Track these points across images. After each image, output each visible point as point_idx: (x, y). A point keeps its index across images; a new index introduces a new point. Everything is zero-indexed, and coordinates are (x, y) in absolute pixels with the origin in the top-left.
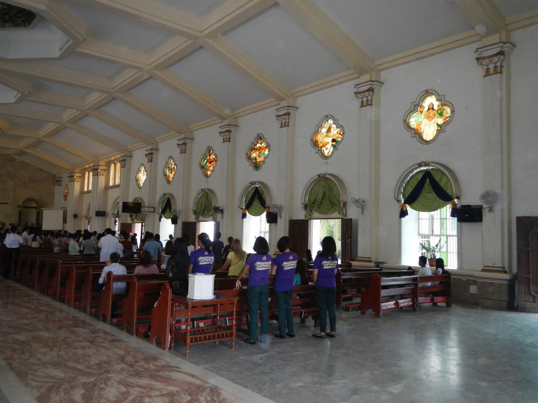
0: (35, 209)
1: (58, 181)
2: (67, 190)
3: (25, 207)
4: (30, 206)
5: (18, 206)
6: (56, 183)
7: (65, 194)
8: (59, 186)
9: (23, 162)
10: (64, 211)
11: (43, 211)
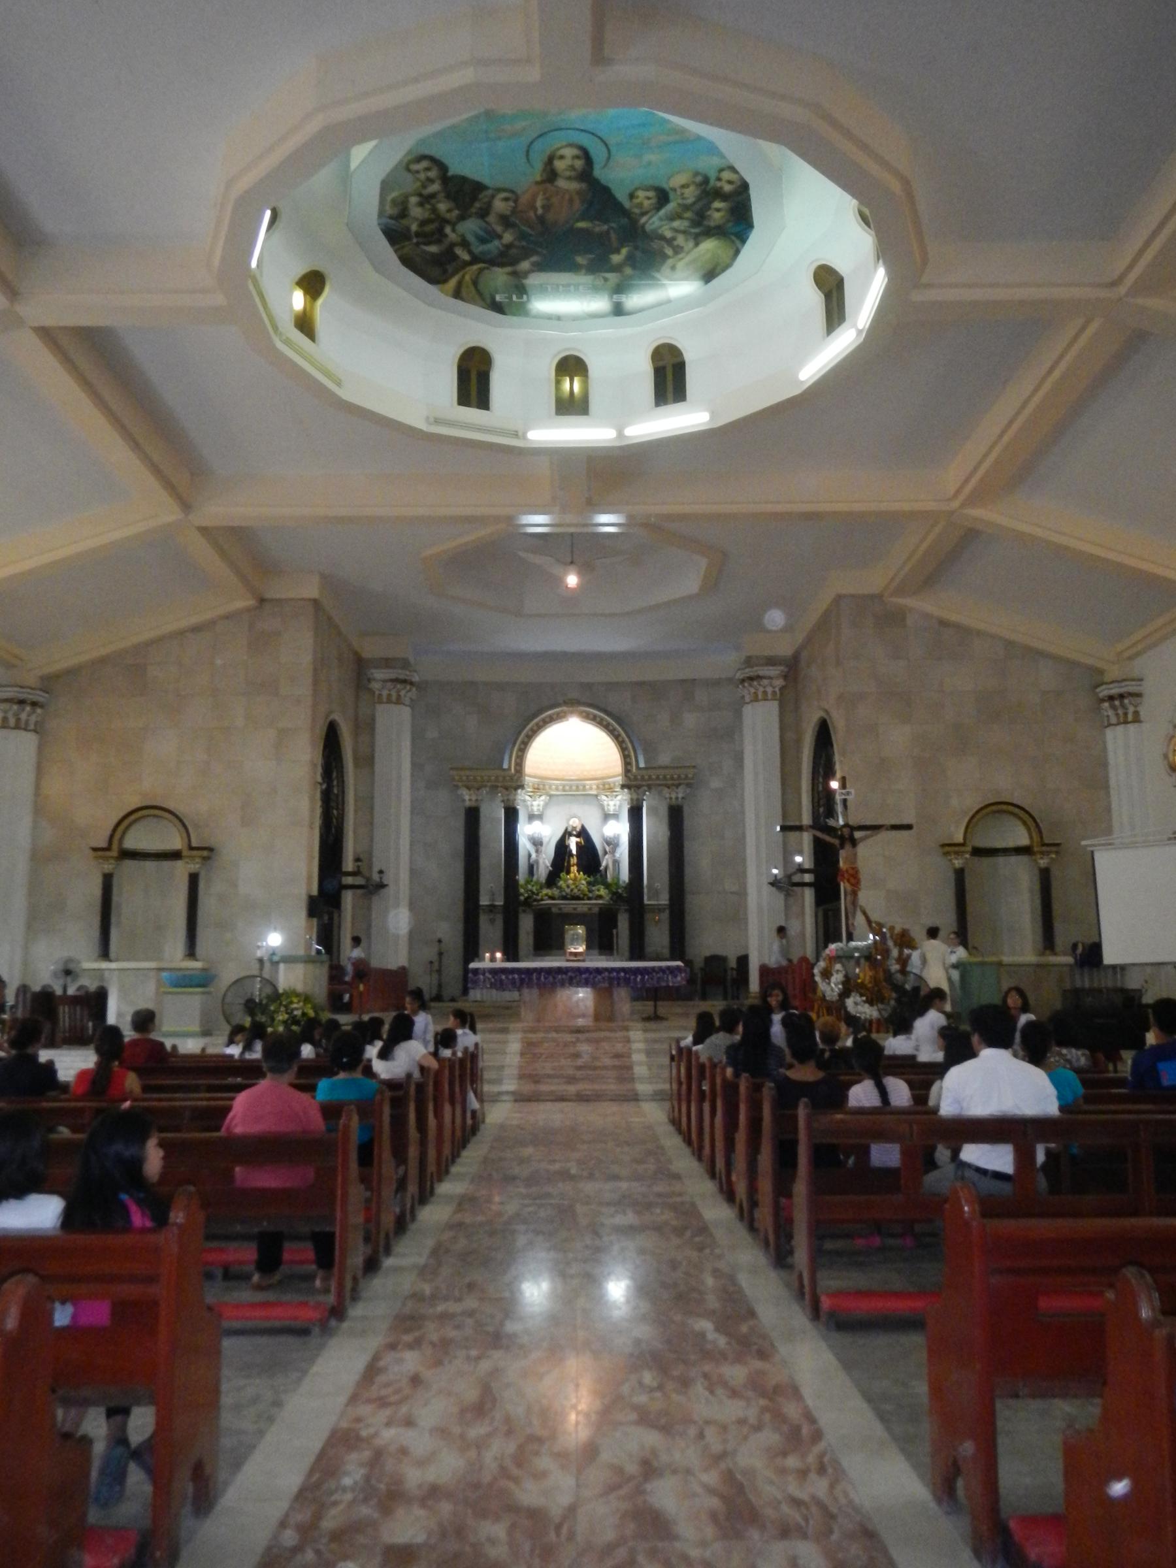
0: (1024, 859)
1: (1122, 696)
3: (978, 852)
4: (999, 844)
5: (943, 846)
6: (1111, 713)
8: (1132, 728)
9: (943, 623)
11: (1092, 852)
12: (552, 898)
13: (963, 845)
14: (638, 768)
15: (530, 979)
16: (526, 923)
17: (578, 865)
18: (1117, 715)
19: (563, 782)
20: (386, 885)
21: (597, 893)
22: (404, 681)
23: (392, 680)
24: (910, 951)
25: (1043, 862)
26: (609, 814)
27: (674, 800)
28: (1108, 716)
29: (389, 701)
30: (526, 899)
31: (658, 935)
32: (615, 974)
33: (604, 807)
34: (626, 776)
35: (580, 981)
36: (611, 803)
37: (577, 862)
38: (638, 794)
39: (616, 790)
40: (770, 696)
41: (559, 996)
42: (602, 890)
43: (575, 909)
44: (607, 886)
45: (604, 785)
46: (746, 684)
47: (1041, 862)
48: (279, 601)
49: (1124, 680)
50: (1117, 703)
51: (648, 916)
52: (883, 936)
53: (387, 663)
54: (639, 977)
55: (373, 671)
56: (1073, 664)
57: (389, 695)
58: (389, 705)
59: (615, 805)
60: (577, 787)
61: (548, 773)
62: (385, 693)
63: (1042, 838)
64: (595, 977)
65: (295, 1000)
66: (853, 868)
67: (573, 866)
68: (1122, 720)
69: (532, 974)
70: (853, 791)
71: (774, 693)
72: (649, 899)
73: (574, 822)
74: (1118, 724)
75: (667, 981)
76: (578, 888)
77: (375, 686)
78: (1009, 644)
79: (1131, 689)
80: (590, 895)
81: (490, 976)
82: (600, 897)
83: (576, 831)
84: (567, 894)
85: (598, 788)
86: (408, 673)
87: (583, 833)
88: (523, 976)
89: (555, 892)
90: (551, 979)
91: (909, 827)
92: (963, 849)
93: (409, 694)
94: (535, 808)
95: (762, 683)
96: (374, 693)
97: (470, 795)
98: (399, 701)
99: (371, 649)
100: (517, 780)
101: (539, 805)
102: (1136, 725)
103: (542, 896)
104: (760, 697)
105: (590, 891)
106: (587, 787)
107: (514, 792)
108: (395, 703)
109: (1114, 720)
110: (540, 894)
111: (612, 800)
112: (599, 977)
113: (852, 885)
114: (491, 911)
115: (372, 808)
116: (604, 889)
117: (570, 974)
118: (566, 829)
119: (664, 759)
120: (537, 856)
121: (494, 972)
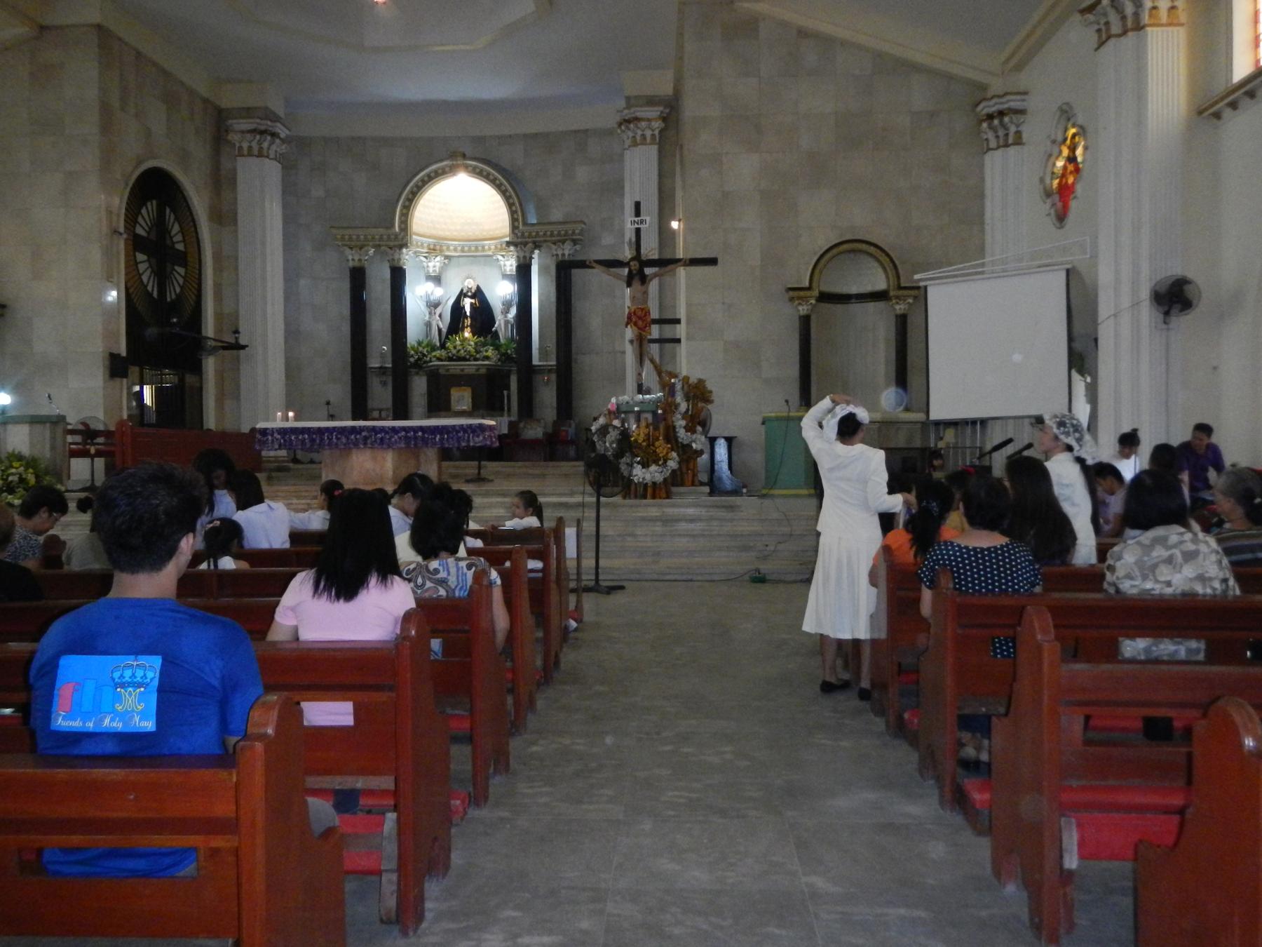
0: (881, 305)
1: (1001, 114)
2: (1066, 152)
3: (825, 298)
4: (854, 290)
6: (990, 135)
7: (1056, 182)
8: (1012, 151)
9: (803, 33)
10: (1068, 271)
11: (926, 287)
12: (439, 359)
13: (809, 288)
14: (525, 224)
15: (322, 440)
16: (419, 386)
17: (471, 326)
18: (997, 137)
20: (247, 346)
21: (485, 354)
22: (262, 133)
23: (253, 131)
24: (703, 404)
25: (900, 308)
27: (560, 256)
28: (987, 140)
29: (250, 154)
30: (417, 361)
31: (547, 396)
32: (412, 433)
35: (375, 441)
36: (508, 263)
38: (525, 252)
40: (648, 139)
41: (354, 457)
42: (490, 351)
43: (462, 370)
44: (497, 347)
46: (623, 127)
47: (897, 307)
48: (61, 28)
49: (1006, 94)
50: (996, 122)
51: (540, 380)
52: (670, 390)
53: (248, 112)
54: (438, 437)
55: (230, 121)
56: (950, 78)
57: (250, 148)
58: (251, 160)
60: (477, 247)
61: (447, 234)
62: (245, 145)
63: (898, 277)
64: (393, 437)
65: (15, 464)
66: (642, 310)
67: (467, 327)
68: (1001, 142)
69: (324, 434)
70: (648, 219)
71: (653, 135)
72: (540, 361)
74: (998, 147)
75: (468, 441)
77: (234, 137)
78: (879, 56)
79: (1013, 105)
80: (478, 356)
81: (279, 437)
82: (487, 358)
83: (471, 292)
84: (454, 355)
86: (269, 123)
87: (478, 294)
88: (314, 436)
89: (443, 353)
90: (344, 440)
91: (712, 262)
92: (808, 293)
93: (274, 147)
94: (431, 270)
95: (639, 125)
96: (234, 144)
97: (352, 255)
98: (260, 155)
99: (230, 99)
100: (403, 239)
101: (434, 267)
102: (1017, 148)
103: (431, 358)
104: (638, 141)
105: (477, 352)
106: (486, 247)
107: (398, 251)
108: (257, 157)
109: (993, 144)
110: (429, 356)
111: (507, 260)
112: (396, 437)
113: (639, 328)
114: (384, 373)
115: (236, 268)
116: (492, 350)
117: (364, 434)
118: (462, 290)
119: (557, 215)
120: (430, 318)
121: (284, 432)
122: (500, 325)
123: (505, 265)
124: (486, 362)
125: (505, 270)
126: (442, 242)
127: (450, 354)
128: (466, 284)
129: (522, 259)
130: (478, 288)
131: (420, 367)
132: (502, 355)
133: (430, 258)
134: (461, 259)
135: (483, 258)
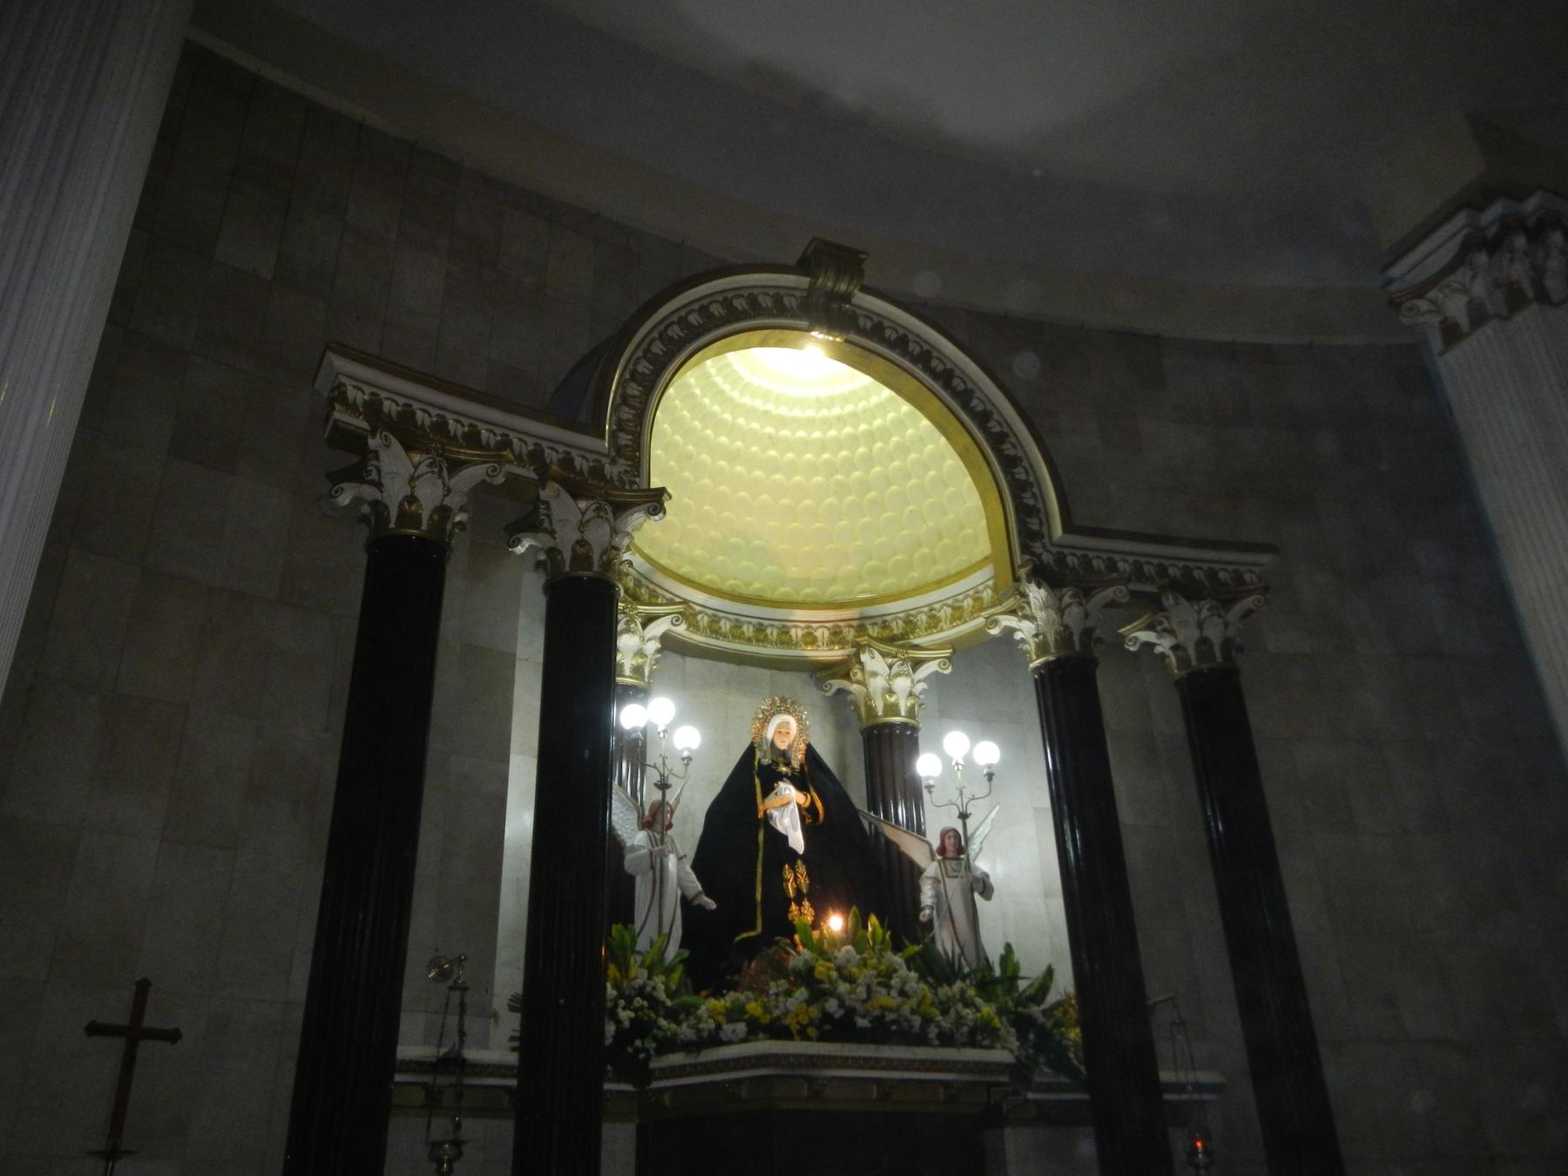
14: (1068, 526)
19: (715, 602)
26: (892, 726)
30: (623, 1036)
33: (868, 697)
34: (1025, 549)
36: (902, 684)
37: (811, 886)
39: (916, 641)
42: (979, 1001)
45: (861, 629)
59: (911, 694)
60: (760, 629)
67: (799, 899)
73: (782, 730)
76: (895, 982)
83: (788, 764)
84: (851, 1012)
85: (836, 637)
87: (811, 774)
101: (640, 653)
106: (797, 633)
107: (610, 515)
111: (898, 675)
114: (432, 1102)
118: (751, 751)
122: (937, 896)
123: (891, 692)
124: (999, 1055)
125: (892, 709)
126: (659, 578)
127: (832, 1005)
128: (770, 733)
129: (1076, 638)
130: (810, 753)
131: (640, 1073)
132: (1022, 1024)
133: (632, 620)
134: (689, 660)
135: (767, 672)
